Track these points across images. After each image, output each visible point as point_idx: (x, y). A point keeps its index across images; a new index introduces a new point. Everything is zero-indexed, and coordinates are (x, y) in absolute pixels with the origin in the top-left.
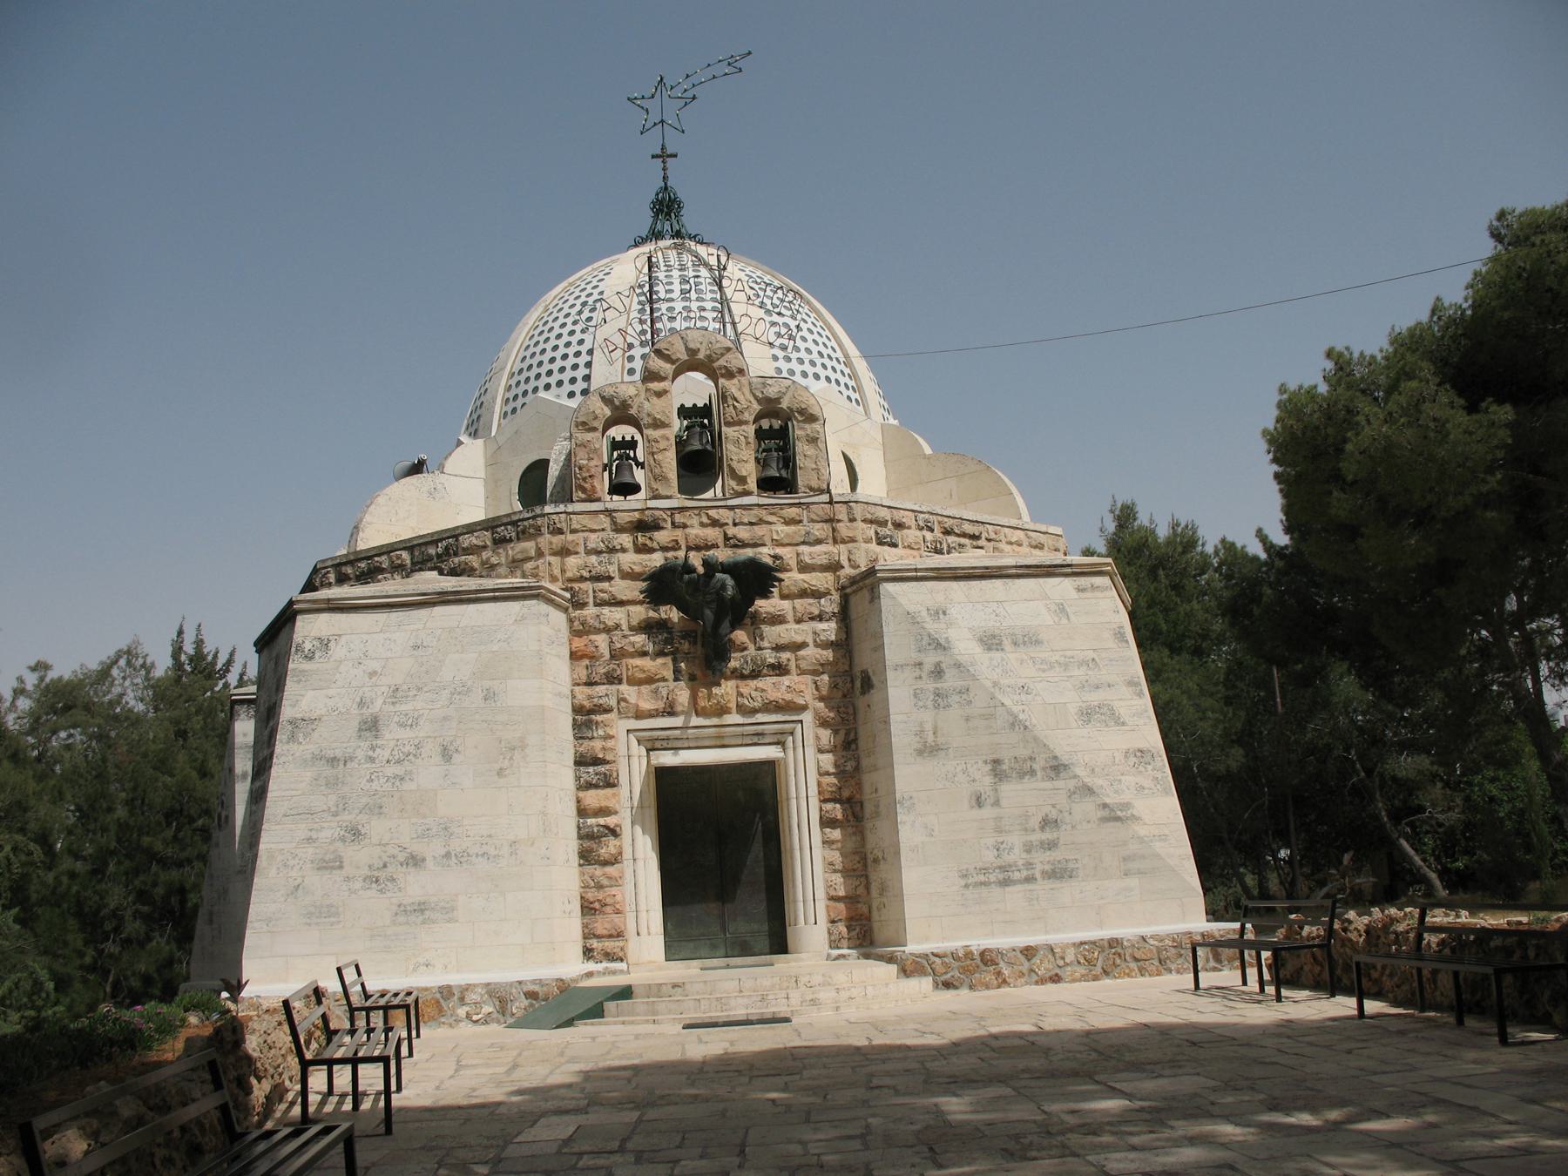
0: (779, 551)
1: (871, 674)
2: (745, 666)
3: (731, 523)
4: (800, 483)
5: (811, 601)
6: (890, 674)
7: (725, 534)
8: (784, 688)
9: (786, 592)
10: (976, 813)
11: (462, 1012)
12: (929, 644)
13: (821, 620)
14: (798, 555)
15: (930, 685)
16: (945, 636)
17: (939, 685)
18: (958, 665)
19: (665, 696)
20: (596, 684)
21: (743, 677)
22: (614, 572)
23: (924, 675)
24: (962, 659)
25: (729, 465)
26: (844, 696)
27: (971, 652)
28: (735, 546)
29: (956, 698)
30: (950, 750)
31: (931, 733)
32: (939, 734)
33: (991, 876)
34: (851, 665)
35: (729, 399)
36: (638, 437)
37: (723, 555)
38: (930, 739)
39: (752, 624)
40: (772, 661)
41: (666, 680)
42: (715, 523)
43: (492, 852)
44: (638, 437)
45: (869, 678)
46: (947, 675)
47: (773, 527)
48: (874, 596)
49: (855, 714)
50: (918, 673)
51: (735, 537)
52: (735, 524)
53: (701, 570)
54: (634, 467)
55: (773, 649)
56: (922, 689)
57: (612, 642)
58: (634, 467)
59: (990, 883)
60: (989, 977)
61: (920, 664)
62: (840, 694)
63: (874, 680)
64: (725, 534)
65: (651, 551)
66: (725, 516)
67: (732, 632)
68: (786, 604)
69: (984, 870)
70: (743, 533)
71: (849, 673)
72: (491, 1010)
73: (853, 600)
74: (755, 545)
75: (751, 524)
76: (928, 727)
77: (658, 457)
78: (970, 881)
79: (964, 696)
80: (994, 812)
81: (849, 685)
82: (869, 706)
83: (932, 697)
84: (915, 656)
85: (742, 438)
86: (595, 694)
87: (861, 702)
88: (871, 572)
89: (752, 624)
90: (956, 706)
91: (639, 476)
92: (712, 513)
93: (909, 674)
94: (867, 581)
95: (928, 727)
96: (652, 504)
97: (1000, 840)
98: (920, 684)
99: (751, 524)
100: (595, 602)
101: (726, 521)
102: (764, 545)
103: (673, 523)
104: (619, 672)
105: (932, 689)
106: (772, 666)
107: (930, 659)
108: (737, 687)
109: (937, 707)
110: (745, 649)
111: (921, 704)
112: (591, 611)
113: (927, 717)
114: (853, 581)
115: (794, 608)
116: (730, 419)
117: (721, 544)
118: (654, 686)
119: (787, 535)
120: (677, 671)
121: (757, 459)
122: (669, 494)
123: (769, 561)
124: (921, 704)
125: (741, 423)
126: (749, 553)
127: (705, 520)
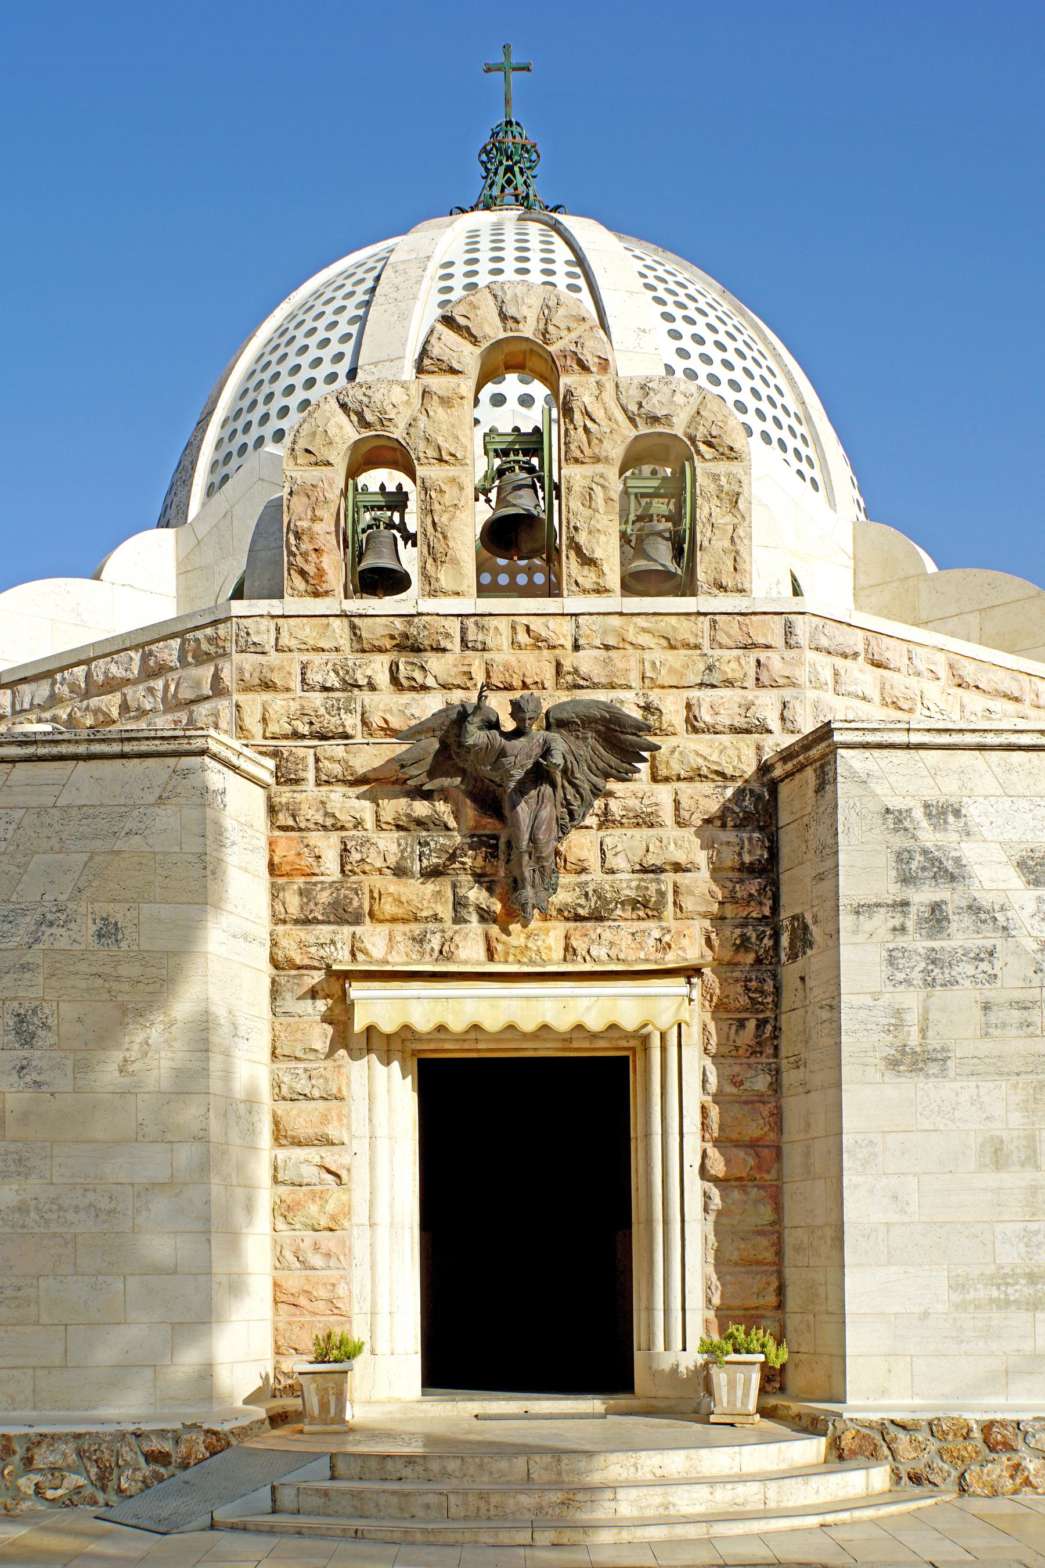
0: (655, 697)
1: (809, 920)
2: (582, 901)
3: (569, 645)
4: (701, 575)
5: (707, 787)
6: (846, 921)
7: (559, 665)
8: (651, 942)
9: (663, 772)
10: (992, 1179)
11: (26, 1483)
12: (924, 869)
13: (724, 826)
14: (689, 706)
15: (918, 944)
16: (953, 854)
17: (936, 944)
18: (974, 909)
19: (437, 948)
20: (316, 921)
21: (578, 918)
22: (355, 726)
23: (910, 924)
24: (985, 900)
25: (571, 539)
26: (759, 961)
27: (1002, 886)
28: (578, 687)
29: (970, 969)
30: (949, 1062)
31: (915, 1031)
32: (930, 1034)
33: (1010, 1290)
34: (775, 909)
35: (577, 416)
36: (408, 485)
37: (552, 699)
38: (914, 1040)
39: (599, 828)
40: (633, 894)
41: (441, 920)
42: (539, 642)
43: (105, 1204)
44: (408, 485)
45: (806, 928)
46: (954, 926)
47: (648, 656)
48: (826, 780)
49: (778, 990)
50: (897, 922)
51: (576, 671)
52: (577, 647)
53: (509, 725)
54: (400, 543)
55: (633, 872)
56: (904, 950)
57: (346, 850)
58: (400, 543)
59: (1008, 1303)
60: (998, 1469)
61: (905, 904)
62: (750, 958)
63: (816, 931)
64: (559, 665)
65: (424, 688)
66: (562, 631)
67: (559, 839)
68: (664, 794)
69: (1002, 1279)
70: (587, 662)
71: (772, 921)
72: (82, 1481)
73: (785, 790)
74: (612, 686)
75: (607, 647)
76: (912, 1018)
77: (442, 519)
78: (969, 1297)
79: (983, 966)
80: (1028, 1176)
81: (767, 942)
82: (802, 979)
83: (923, 965)
84: (891, 890)
85: (598, 490)
86: (312, 940)
87: (789, 973)
88: (825, 732)
89: (599, 828)
90: (967, 983)
91: (409, 559)
92: (536, 624)
93: (881, 922)
94: (814, 753)
95: (912, 1018)
96: (428, 605)
97: (1033, 1226)
98: (902, 941)
99: (607, 647)
100: (317, 778)
101: (562, 642)
102: (630, 687)
103: (464, 642)
104: (356, 903)
105: (922, 951)
106: (634, 904)
107: (922, 896)
108: (567, 937)
109: (930, 983)
110: (584, 870)
111: (900, 976)
112: (309, 793)
113: (911, 1000)
114: (786, 755)
115: (677, 803)
116: (577, 454)
117: (549, 683)
118: (416, 928)
119: (672, 670)
120: (459, 903)
121: (624, 536)
122: (459, 589)
123: (637, 714)
124: (900, 976)
125: (597, 460)
126: (602, 696)
127: (523, 638)
